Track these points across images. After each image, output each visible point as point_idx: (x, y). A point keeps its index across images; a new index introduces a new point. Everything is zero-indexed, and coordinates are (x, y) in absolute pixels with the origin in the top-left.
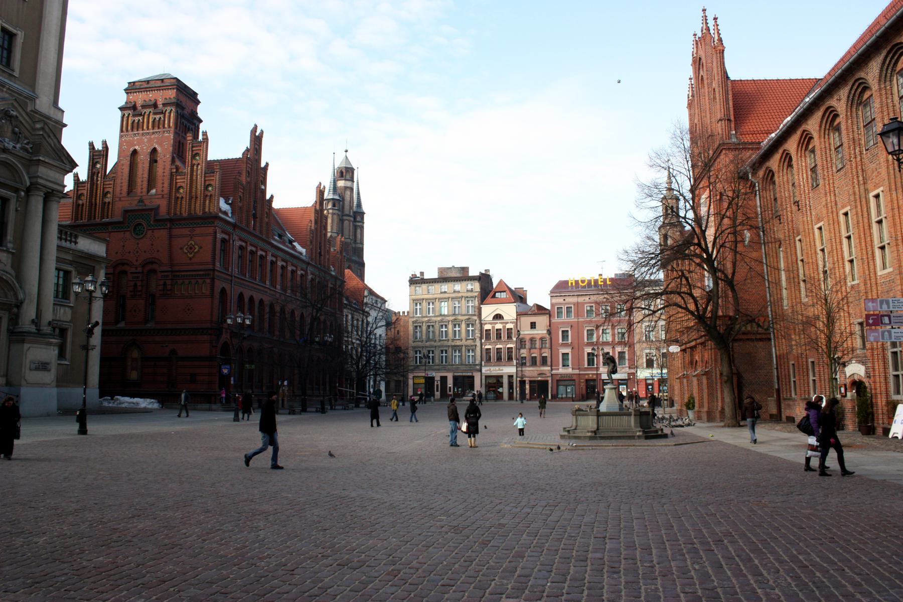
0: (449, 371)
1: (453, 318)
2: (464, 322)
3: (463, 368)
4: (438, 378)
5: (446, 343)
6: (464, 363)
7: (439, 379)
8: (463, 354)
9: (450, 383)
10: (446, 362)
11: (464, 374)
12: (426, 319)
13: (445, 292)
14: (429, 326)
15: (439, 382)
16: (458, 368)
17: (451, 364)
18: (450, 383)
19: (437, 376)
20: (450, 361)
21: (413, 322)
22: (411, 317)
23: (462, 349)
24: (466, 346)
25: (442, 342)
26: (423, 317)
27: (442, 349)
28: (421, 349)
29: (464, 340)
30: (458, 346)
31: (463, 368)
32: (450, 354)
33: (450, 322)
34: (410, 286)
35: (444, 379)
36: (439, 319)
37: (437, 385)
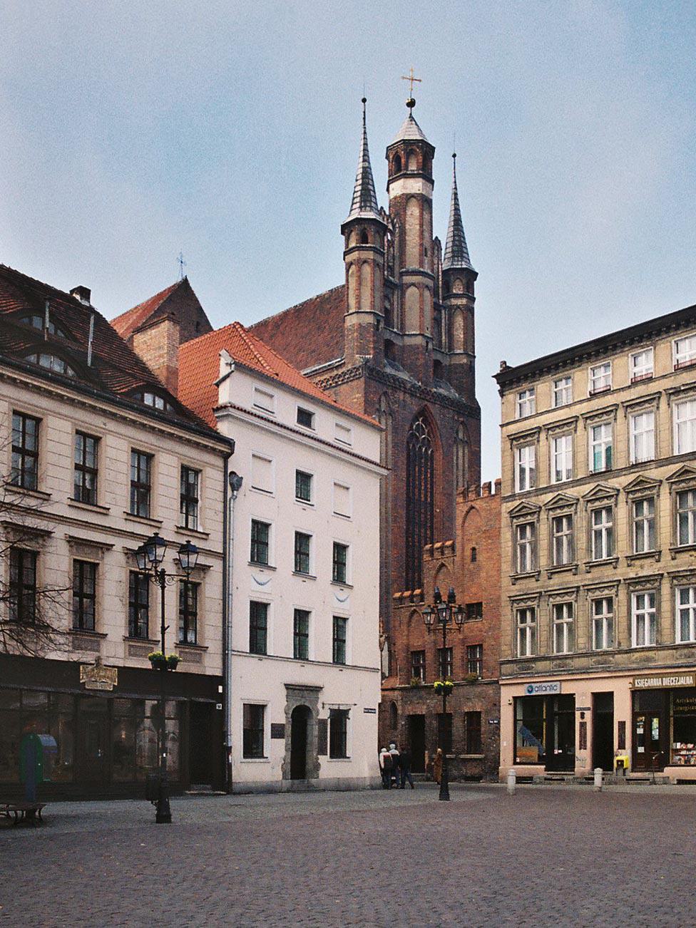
0: (616, 672)
1: (632, 477)
2: (665, 490)
3: (663, 658)
4: (583, 701)
5: (608, 574)
6: (667, 641)
7: (588, 702)
8: (666, 606)
9: (622, 710)
10: (611, 641)
11: (668, 682)
12: (549, 497)
13: (607, 392)
14: (558, 520)
15: (588, 715)
16: (648, 659)
17: (624, 647)
18: (622, 710)
19: (583, 692)
20: (623, 636)
21: (513, 515)
22: (506, 499)
23: (659, 590)
24: (674, 576)
25: (596, 572)
26: (539, 491)
27: (598, 594)
28: (533, 604)
29: (666, 556)
30: (648, 579)
31: (663, 658)
32: (624, 609)
33: (622, 497)
34: (502, 393)
35: (603, 702)
36: (586, 488)
37: (583, 725)
